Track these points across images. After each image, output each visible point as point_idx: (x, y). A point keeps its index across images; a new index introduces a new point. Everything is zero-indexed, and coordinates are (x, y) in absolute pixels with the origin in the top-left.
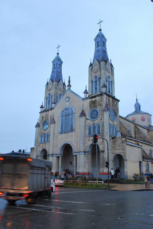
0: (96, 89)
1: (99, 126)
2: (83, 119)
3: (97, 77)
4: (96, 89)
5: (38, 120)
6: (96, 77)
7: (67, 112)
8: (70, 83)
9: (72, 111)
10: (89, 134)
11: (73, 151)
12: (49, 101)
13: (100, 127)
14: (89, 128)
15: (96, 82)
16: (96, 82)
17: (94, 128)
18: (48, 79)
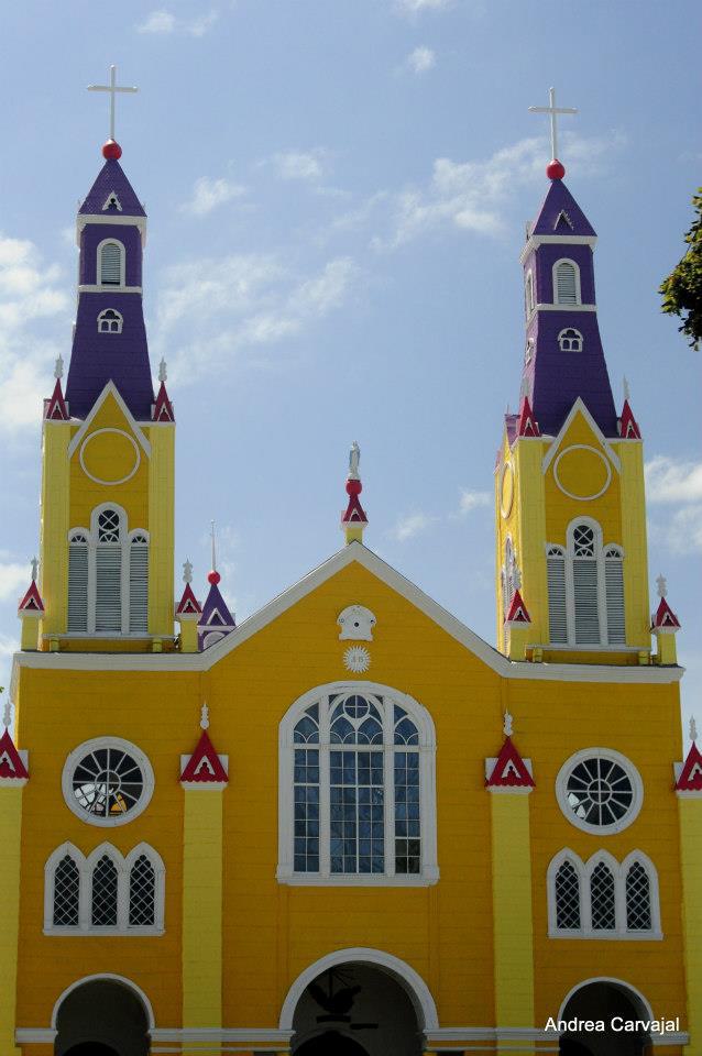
0: (586, 609)
1: (637, 878)
2: (510, 802)
3: (590, 535)
4: (586, 609)
5: (7, 721)
6: (584, 536)
7: (356, 723)
8: (362, 498)
9: (406, 731)
10: (561, 916)
11: (431, 1025)
12: (109, 578)
13: (644, 880)
14: (560, 880)
15: (585, 570)
16: (585, 570)
17: (602, 879)
18: (60, 362)
